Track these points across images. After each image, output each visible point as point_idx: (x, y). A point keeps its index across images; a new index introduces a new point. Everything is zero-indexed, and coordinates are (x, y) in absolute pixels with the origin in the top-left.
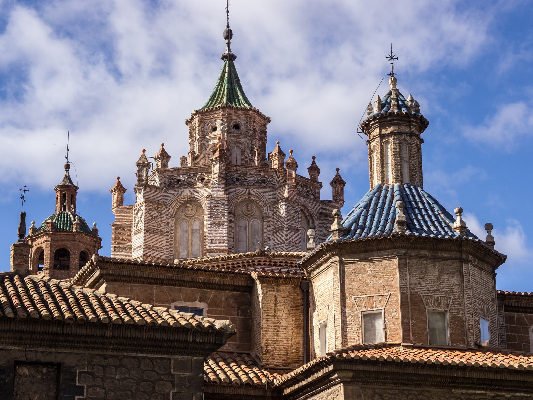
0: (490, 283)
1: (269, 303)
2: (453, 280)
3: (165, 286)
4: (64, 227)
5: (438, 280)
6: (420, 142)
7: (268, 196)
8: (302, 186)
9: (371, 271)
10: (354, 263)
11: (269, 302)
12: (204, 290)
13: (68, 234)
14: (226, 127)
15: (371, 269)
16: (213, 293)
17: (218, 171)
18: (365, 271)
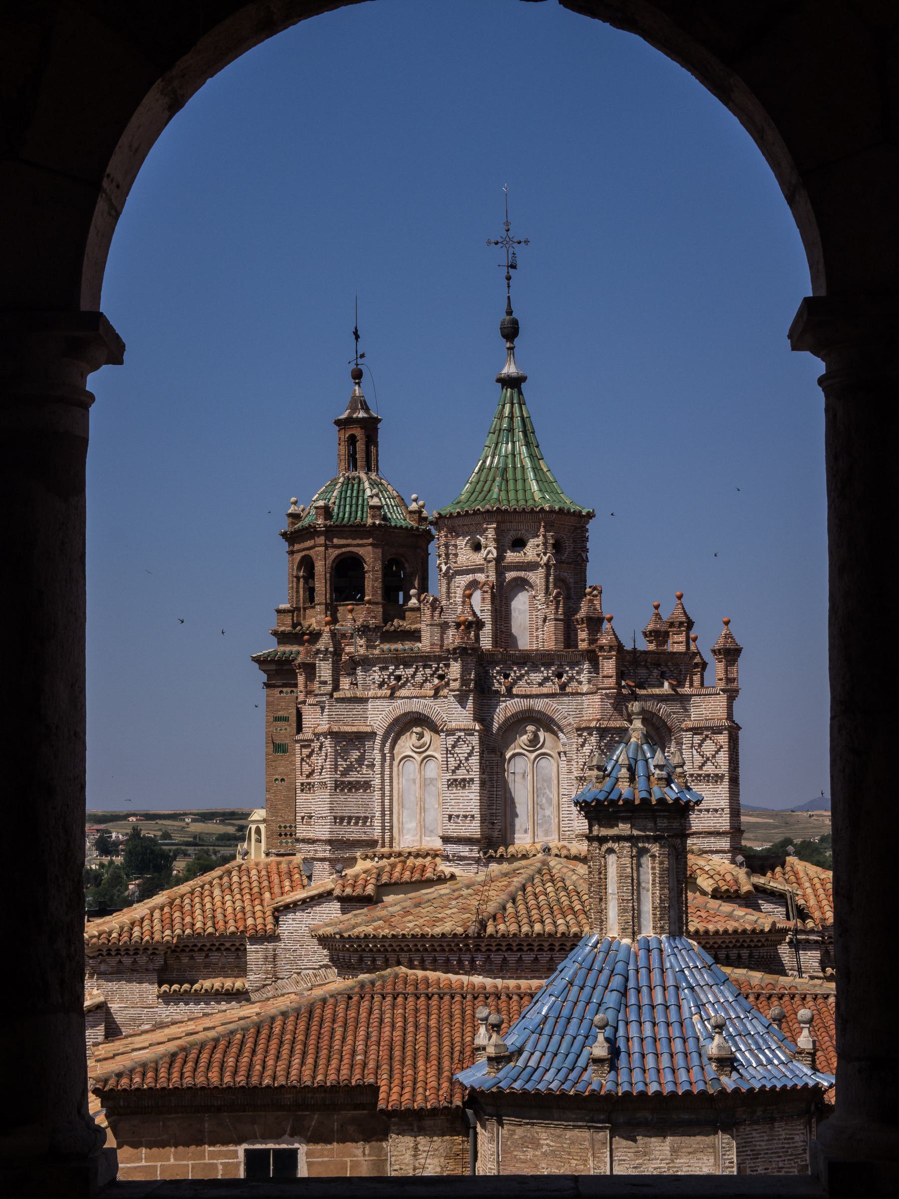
0: (797, 1138)
1: (404, 1155)
2: (700, 1165)
3: (225, 1114)
4: (350, 514)
5: (670, 1167)
6: (681, 839)
7: (567, 710)
8: (648, 668)
9: (548, 1145)
10: (520, 1125)
11: (404, 1152)
12: (300, 1113)
13: (358, 529)
14: (495, 552)
15: (548, 1141)
16: (316, 1117)
17: (458, 676)
18: (537, 1145)
